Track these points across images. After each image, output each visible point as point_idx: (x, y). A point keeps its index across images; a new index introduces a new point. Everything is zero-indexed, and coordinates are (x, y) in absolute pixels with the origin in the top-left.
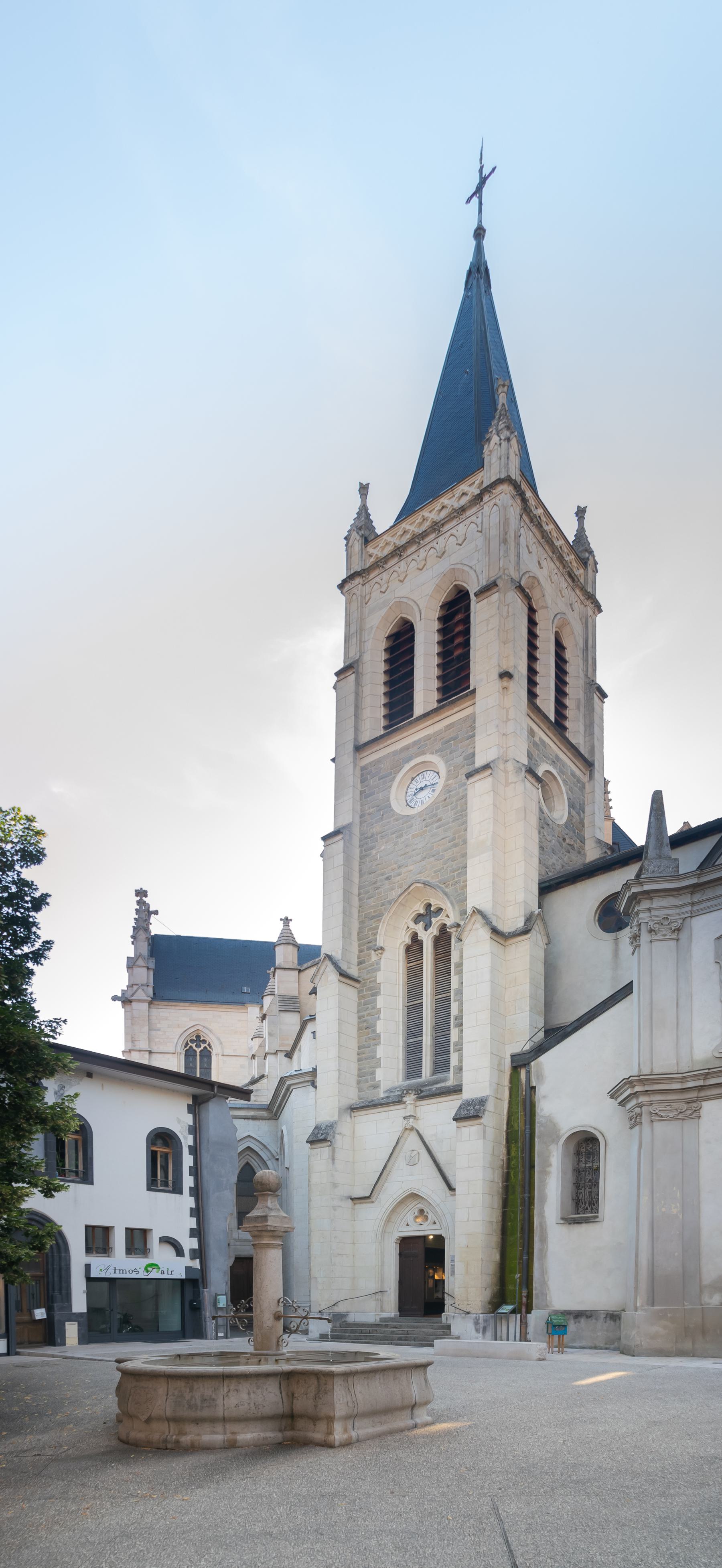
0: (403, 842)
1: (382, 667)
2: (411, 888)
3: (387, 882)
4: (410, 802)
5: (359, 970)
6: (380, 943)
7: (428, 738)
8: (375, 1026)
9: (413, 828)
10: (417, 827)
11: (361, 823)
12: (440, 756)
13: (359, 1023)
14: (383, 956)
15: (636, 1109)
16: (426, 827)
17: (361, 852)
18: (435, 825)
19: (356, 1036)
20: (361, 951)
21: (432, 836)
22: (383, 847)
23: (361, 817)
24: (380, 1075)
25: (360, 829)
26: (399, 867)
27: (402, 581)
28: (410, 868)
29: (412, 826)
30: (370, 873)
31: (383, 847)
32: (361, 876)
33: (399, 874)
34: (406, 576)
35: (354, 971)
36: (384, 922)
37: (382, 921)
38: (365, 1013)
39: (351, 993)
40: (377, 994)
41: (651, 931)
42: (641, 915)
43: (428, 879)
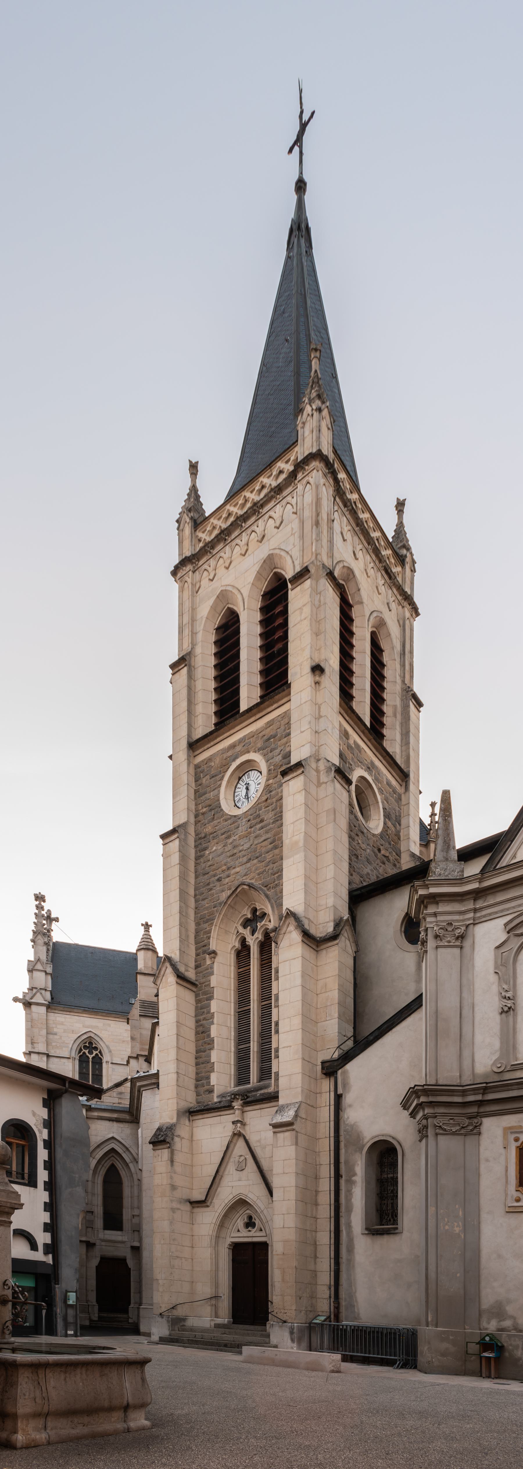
0: (232, 843)
1: (212, 661)
2: (238, 890)
3: (218, 884)
4: (237, 802)
5: (196, 973)
6: (213, 946)
7: (252, 735)
8: (210, 1031)
9: (240, 828)
10: (243, 827)
11: (196, 823)
12: (261, 754)
13: (197, 1027)
14: (216, 960)
16: (251, 827)
17: (196, 852)
18: (258, 826)
19: (194, 1040)
20: (197, 955)
21: (256, 837)
22: (214, 848)
23: (196, 816)
24: (214, 1079)
25: (195, 829)
26: (228, 869)
27: (227, 568)
28: (237, 869)
29: (238, 827)
30: (205, 874)
31: (214, 848)
32: (196, 877)
33: (228, 876)
34: (231, 562)
35: (191, 974)
36: (216, 925)
37: (214, 924)
38: (201, 1017)
39: (189, 997)
40: (211, 998)
43: (253, 881)
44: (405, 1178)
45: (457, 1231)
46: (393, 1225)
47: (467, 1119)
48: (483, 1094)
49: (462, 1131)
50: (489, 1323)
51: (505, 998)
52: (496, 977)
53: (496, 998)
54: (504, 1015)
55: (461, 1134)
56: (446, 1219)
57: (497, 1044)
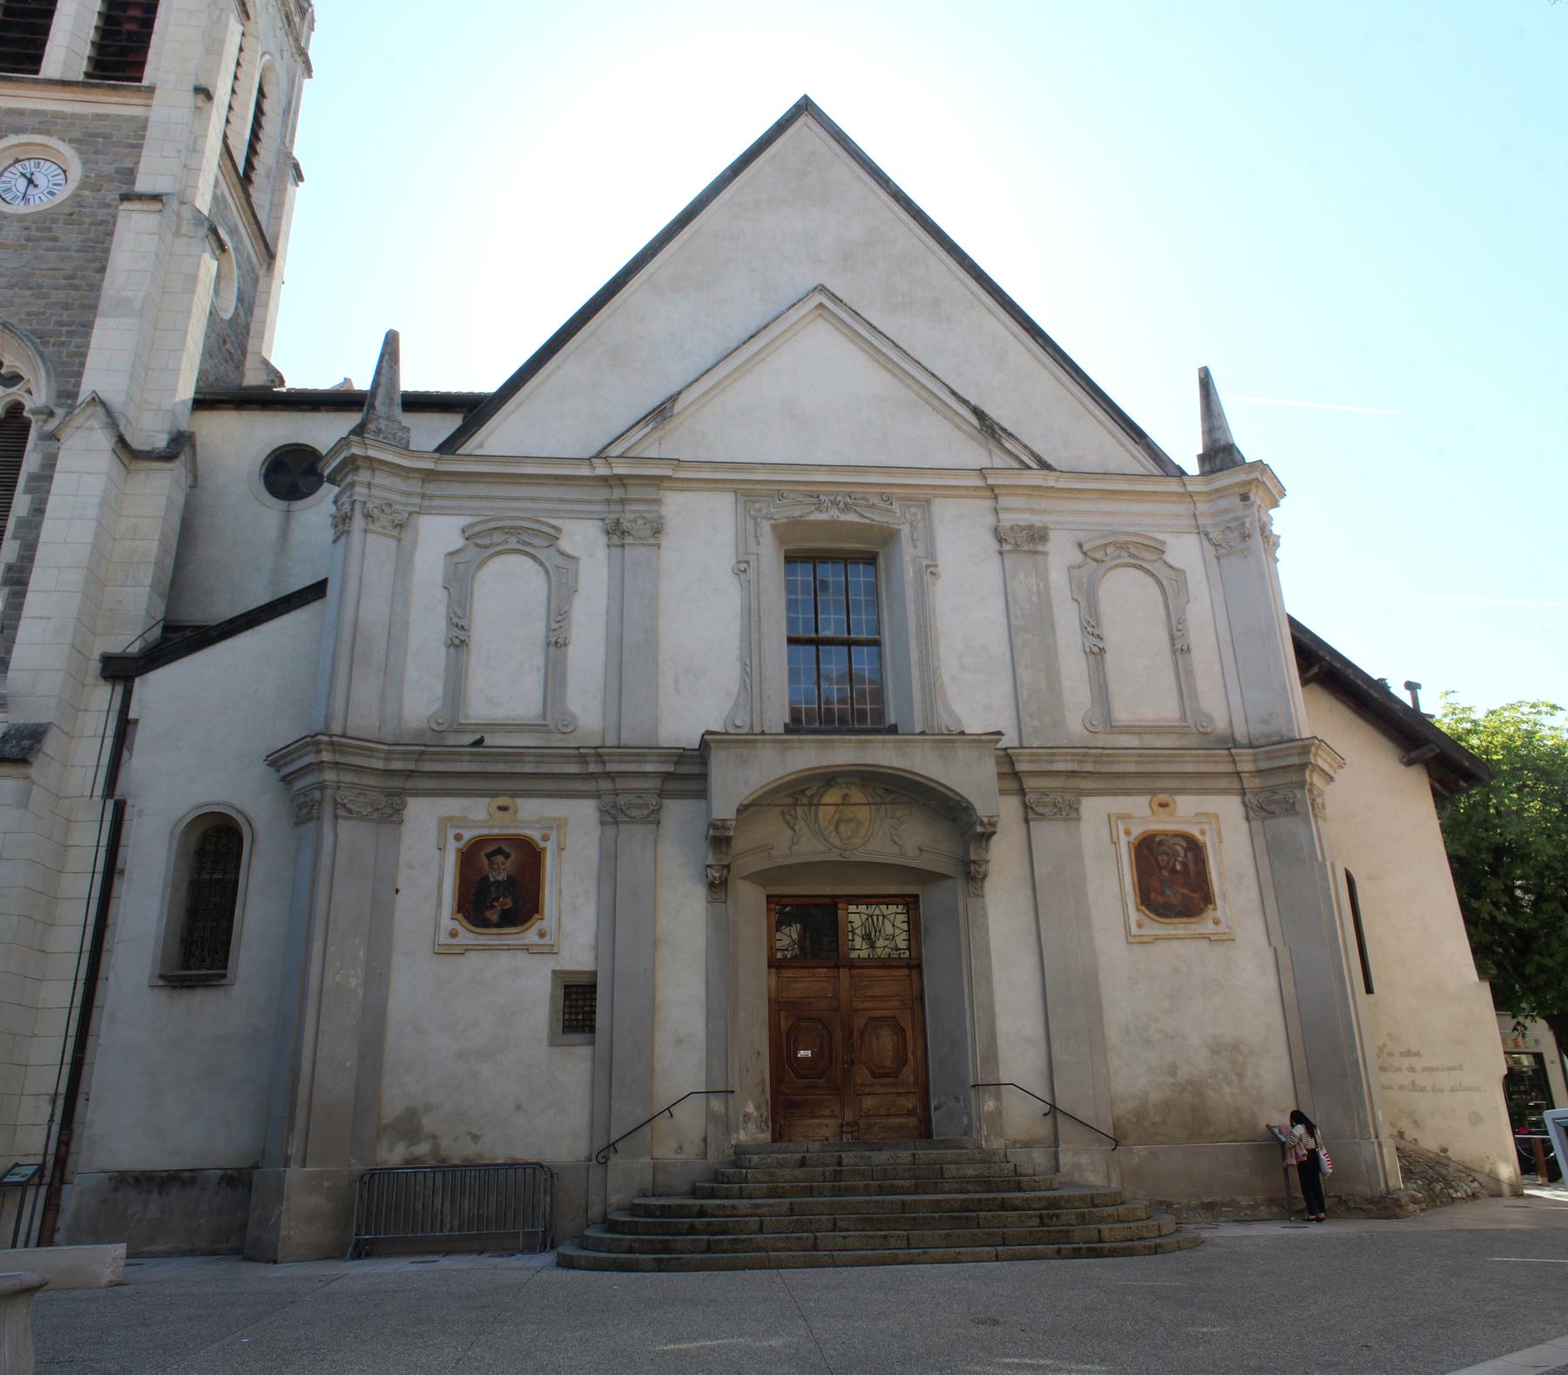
41: (368, 516)
42: (358, 489)
44: (251, 884)
46: (211, 969)
47: (386, 796)
48: (417, 761)
49: (375, 816)
50: (391, 1150)
51: (457, 626)
52: (445, 593)
53: (443, 624)
54: (452, 650)
55: (374, 820)
57: (438, 687)
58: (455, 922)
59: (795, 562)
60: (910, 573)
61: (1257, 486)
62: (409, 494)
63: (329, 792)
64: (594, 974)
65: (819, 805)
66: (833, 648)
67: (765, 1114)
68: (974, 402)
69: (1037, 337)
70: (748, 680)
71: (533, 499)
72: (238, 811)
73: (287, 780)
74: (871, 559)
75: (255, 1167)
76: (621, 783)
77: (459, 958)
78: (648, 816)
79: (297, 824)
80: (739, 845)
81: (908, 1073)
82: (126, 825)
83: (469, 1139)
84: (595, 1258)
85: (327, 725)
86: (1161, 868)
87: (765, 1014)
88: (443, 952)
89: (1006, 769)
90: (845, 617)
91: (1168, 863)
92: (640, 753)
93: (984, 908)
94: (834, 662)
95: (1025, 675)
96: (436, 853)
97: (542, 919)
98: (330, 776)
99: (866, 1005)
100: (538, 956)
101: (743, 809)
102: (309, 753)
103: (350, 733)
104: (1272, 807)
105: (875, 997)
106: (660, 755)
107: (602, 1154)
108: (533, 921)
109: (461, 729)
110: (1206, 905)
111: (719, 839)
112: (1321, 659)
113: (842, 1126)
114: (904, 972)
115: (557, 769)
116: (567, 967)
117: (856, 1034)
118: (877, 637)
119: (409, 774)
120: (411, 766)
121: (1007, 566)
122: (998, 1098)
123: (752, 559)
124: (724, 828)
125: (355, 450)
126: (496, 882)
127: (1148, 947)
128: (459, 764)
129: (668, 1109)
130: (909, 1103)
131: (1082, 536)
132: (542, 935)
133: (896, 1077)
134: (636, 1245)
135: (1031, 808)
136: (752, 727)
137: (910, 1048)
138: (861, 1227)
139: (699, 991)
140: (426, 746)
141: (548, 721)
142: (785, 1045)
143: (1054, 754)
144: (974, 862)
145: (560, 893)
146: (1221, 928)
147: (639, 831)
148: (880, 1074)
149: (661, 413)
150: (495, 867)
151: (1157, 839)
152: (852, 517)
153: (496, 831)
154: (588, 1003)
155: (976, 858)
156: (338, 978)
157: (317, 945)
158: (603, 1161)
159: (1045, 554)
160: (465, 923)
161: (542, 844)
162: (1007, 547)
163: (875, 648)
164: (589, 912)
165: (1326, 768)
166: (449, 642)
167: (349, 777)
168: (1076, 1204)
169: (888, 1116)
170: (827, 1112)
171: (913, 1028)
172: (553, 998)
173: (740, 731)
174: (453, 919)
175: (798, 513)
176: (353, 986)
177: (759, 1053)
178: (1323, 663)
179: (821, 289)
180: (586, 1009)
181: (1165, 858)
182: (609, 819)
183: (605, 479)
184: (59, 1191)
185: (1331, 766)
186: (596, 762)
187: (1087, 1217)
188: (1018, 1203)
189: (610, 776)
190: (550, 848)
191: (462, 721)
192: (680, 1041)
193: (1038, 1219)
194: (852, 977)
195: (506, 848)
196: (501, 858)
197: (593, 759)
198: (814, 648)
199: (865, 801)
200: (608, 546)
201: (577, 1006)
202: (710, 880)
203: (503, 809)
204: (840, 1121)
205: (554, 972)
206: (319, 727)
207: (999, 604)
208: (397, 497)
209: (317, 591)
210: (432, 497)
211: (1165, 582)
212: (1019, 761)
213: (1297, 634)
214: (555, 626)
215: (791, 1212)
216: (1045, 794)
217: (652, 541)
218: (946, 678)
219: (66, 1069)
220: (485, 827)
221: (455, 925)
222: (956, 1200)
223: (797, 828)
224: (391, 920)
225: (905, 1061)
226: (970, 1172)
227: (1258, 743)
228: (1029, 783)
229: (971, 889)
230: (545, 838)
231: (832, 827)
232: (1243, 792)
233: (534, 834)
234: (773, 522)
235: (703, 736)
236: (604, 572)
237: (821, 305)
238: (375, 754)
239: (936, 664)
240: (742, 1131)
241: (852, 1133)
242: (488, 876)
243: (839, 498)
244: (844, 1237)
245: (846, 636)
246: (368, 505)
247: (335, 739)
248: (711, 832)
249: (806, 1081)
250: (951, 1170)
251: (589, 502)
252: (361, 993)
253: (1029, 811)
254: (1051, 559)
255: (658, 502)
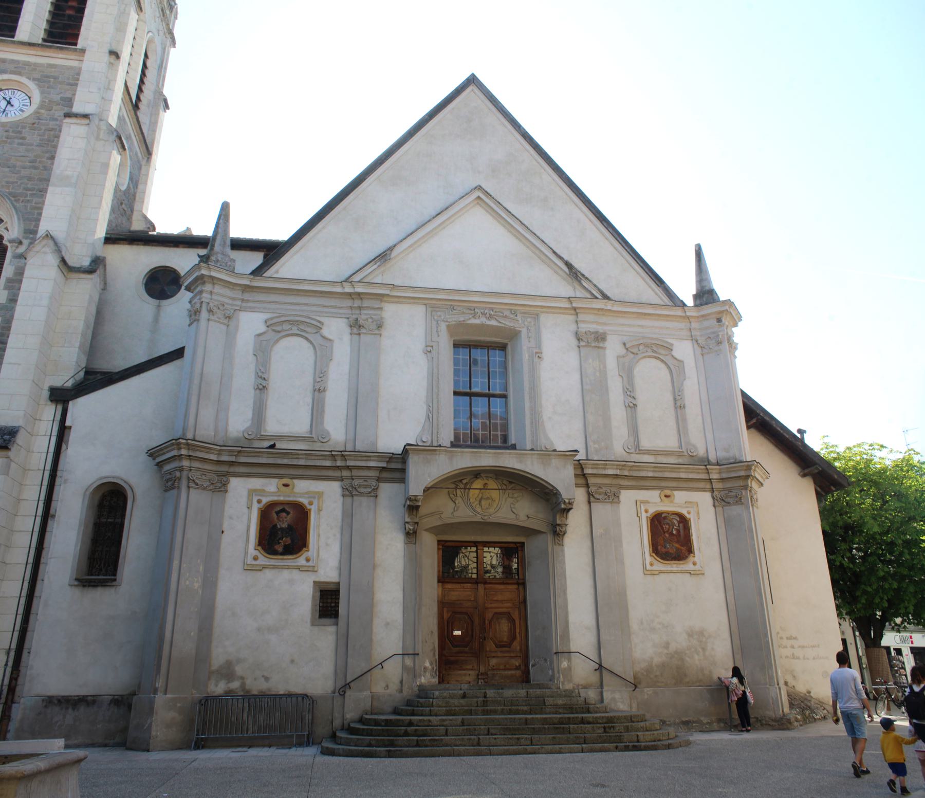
15: (176, 472)
41: (210, 311)
42: (204, 295)
45: (196, 588)
47: (218, 476)
49: (211, 487)
50: (216, 686)
52: (254, 358)
53: (253, 376)
54: (258, 391)
55: (210, 490)
56: (188, 574)
58: (257, 551)
59: (458, 347)
60: (526, 356)
61: (726, 314)
62: (234, 299)
63: (185, 473)
64: (338, 584)
65: (470, 489)
66: (480, 399)
67: (435, 668)
68: (566, 258)
69: (603, 222)
70: (430, 415)
71: (307, 305)
72: (125, 482)
73: (160, 465)
74: (503, 347)
75: (134, 694)
76: (355, 473)
77: (259, 573)
78: (370, 493)
79: (166, 491)
80: (423, 511)
81: (516, 645)
82: (56, 488)
83: (263, 679)
84: (349, 750)
85: (184, 434)
86: (664, 533)
87: (435, 609)
88: (249, 569)
89: (579, 472)
90: (487, 381)
91: (669, 529)
92: (367, 455)
93: (563, 551)
94: (480, 406)
95: (590, 418)
96: (246, 510)
97: (308, 551)
98: (186, 463)
99: (493, 605)
100: (305, 573)
101: (426, 490)
102: (174, 449)
103: (197, 439)
104: (728, 500)
105: (497, 601)
106: (379, 457)
107: (341, 690)
108: (302, 552)
109: (262, 438)
110: (689, 554)
111: (412, 507)
112: (758, 415)
113: (478, 675)
114: (515, 587)
115: (318, 463)
116: (322, 579)
117: (487, 622)
118: (505, 393)
119: (232, 463)
120: (233, 459)
121: (582, 355)
122: (569, 660)
123: (435, 345)
124: (416, 500)
125: (204, 272)
126: (282, 528)
127: (655, 576)
128: (260, 458)
129: (381, 663)
130: (517, 662)
131: (625, 339)
132: (308, 560)
133: (510, 647)
134: (373, 742)
135: (592, 495)
136: (432, 442)
137: (518, 631)
138: (503, 733)
139: (400, 595)
140: (242, 447)
141: (313, 435)
142: (446, 628)
143: (606, 465)
144: (559, 525)
145: (319, 536)
146: (697, 568)
147: (364, 500)
148: (500, 645)
149: (383, 257)
150: (281, 519)
151: (663, 516)
152: (493, 323)
153: (282, 498)
154: (334, 601)
155: (560, 523)
156: (188, 582)
157: (176, 563)
158: (342, 693)
159: (604, 348)
160: (262, 552)
161: (309, 507)
162: (582, 344)
163: (504, 399)
164: (335, 548)
165: (760, 479)
166: (256, 387)
167: (196, 464)
168: (622, 721)
169: (505, 669)
170: (469, 667)
171: (520, 619)
172: (314, 597)
173: (425, 444)
174: (255, 549)
175: (462, 319)
176: (196, 588)
177: (432, 632)
178: (759, 417)
179: (479, 188)
180: (333, 605)
181: (667, 526)
182: (348, 493)
183: (350, 294)
184: (10, 708)
185: (762, 477)
186: (342, 460)
187: (630, 728)
188: (591, 720)
189: (348, 468)
190: (313, 509)
191: (262, 434)
192: (387, 624)
193: (603, 729)
194: (485, 589)
195: (287, 508)
196: (284, 514)
197: (339, 458)
198: (469, 398)
199: (497, 487)
200: (351, 334)
201: (327, 603)
202: (407, 531)
203: (286, 485)
204: (477, 672)
205: (315, 582)
206: (179, 434)
207: (577, 376)
208: (227, 301)
209: (178, 354)
210: (248, 301)
211: (672, 367)
212: (586, 468)
213: (745, 400)
214: (319, 380)
215: (463, 724)
216: (600, 487)
217: (377, 332)
218: (545, 418)
219: (16, 634)
220: (276, 496)
221: (257, 553)
222: (556, 718)
223: (457, 502)
224: (218, 549)
225: (514, 638)
226: (560, 702)
227: (722, 463)
228: (591, 481)
229: (556, 540)
230: (311, 503)
231: (477, 502)
232: (712, 490)
233: (304, 501)
234: (447, 324)
235: (405, 446)
236: (348, 349)
237: (479, 197)
238: (212, 451)
239: (540, 410)
240: (423, 677)
241: (484, 679)
242: (276, 525)
243: (486, 311)
244: (495, 739)
245: (487, 391)
246: (210, 304)
247: (189, 441)
248: (408, 503)
249: (458, 648)
250: (549, 701)
251: (340, 308)
252: (201, 592)
253: (591, 497)
254: (608, 351)
255: (380, 309)
